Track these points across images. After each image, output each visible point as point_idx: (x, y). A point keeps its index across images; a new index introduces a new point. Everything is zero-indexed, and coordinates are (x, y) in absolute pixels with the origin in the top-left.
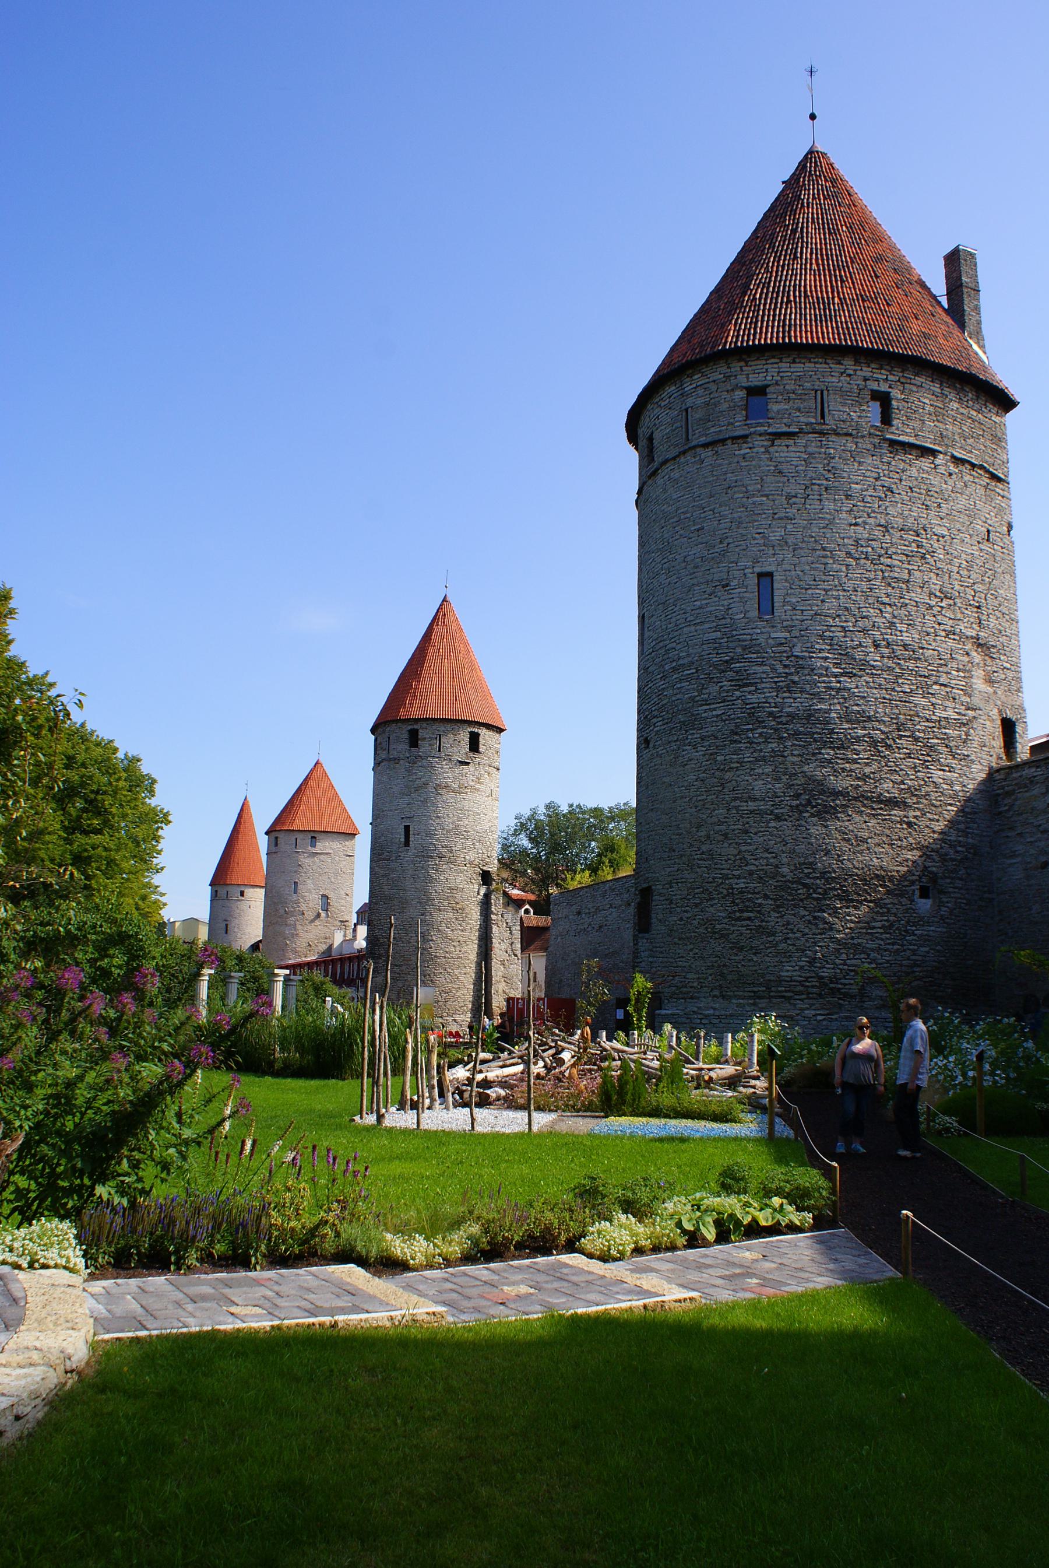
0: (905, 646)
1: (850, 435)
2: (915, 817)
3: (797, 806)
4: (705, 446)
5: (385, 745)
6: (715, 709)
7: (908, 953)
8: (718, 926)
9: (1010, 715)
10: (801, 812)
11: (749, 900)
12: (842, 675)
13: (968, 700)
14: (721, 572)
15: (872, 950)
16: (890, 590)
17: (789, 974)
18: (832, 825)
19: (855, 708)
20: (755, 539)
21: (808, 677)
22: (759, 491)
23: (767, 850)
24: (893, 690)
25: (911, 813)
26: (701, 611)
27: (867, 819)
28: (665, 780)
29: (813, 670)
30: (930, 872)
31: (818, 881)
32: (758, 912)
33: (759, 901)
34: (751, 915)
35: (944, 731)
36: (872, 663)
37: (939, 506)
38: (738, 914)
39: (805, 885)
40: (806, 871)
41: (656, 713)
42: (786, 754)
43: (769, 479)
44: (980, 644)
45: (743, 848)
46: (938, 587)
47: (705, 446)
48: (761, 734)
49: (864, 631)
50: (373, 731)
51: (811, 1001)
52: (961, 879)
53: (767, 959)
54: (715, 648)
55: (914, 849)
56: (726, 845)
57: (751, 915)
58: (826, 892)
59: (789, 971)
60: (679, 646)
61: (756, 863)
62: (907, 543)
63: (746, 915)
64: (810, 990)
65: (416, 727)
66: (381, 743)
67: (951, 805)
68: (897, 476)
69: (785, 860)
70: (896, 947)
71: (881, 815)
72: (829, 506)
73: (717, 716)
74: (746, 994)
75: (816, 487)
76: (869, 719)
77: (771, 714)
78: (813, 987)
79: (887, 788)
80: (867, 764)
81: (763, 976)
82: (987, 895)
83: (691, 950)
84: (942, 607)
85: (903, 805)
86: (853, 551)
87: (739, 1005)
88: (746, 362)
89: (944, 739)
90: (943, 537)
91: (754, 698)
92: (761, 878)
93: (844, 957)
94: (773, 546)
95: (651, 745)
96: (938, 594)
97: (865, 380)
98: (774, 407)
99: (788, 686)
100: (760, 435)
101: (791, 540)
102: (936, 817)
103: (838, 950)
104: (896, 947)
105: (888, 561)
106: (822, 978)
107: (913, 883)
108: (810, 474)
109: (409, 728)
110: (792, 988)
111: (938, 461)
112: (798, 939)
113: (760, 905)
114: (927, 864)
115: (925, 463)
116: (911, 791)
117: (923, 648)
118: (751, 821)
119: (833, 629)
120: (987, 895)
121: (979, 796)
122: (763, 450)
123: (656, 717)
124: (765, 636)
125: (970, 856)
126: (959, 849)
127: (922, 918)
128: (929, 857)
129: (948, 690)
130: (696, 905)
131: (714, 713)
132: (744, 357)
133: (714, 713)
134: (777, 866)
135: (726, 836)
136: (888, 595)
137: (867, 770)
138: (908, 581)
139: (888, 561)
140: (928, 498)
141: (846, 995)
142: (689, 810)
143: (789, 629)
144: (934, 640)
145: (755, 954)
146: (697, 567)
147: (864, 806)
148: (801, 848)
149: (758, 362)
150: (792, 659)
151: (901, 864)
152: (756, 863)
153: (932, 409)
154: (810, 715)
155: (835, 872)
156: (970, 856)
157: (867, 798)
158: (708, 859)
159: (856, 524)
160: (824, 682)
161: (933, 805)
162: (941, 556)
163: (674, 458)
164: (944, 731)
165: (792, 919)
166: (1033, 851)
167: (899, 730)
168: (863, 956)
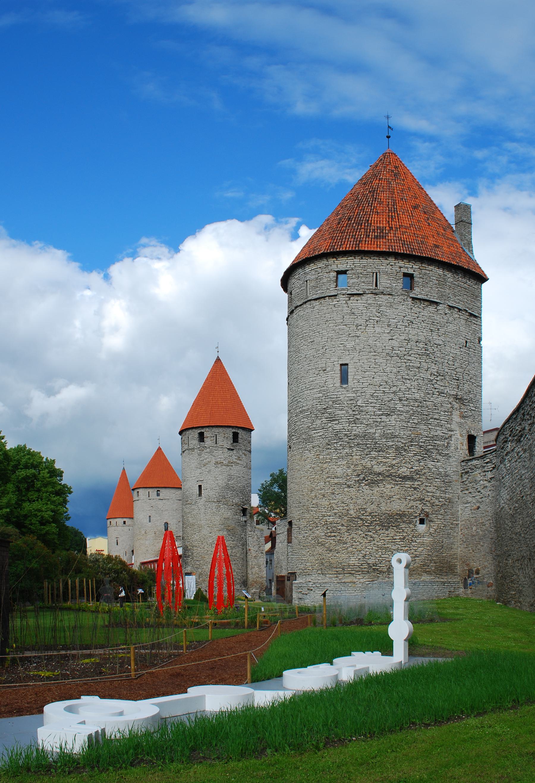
0: (416, 400)
2: (418, 485)
3: (358, 480)
5: (186, 442)
7: (412, 551)
8: (320, 540)
9: (473, 433)
10: (360, 483)
11: (334, 527)
12: (382, 415)
13: (449, 426)
15: (394, 550)
17: (353, 562)
18: (376, 489)
19: (388, 431)
20: (340, 347)
21: (365, 416)
22: (342, 323)
23: (343, 503)
24: (408, 422)
25: (416, 483)
27: (393, 486)
28: (297, 467)
29: (367, 413)
30: (426, 512)
31: (368, 517)
32: (339, 533)
33: (339, 527)
34: (336, 534)
35: (435, 442)
36: (398, 409)
38: (329, 534)
39: (361, 519)
40: (362, 512)
42: (353, 455)
43: (348, 316)
44: (456, 397)
45: (332, 502)
48: (341, 445)
49: (394, 393)
50: (181, 433)
51: (364, 575)
52: (442, 515)
53: (343, 555)
55: (417, 500)
56: (324, 500)
57: (336, 534)
58: (372, 522)
59: (353, 561)
60: (303, 400)
61: (338, 509)
63: (333, 534)
64: (363, 570)
65: (202, 431)
66: (184, 441)
67: (437, 478)
69: (352, 507)
70: (406, 548)
71: (400, 484)
72: (378, 330)
74: (333, 572)
76: (396, 436)
77: (346, 434)
78: (365, 568)
79: (404, 471)
80: (394, 459)
81: (341, 563)
82: (454, 522)
83: (308, 552)
85: (411, 478)
86: (390, 353)
87: (330, 578)
89: (435, 446)
91: (337, 427)
92: (340, 516)
93: (380, 553)
94: (349, 351)
99: (354, 421)
100: (343, 295)
101: (358, 348)
102: (430, 485)
103: (377, 550)
104: (406, 548)
106: (369, 564)
107: (416, 517)
108: (369, 314)
109: (199, 431)
110: (354, 569)
112: (357, 545)
113: (340, 529)
114: (423, 508)
116: (417, 472)
117: (425, 401)
118: (336, 488)
119: (377, 392)
120: (454, 522)
121: (453, 474)
122: (344, 302)
123: (293, 436)
124: (344, 396)
125: (446, 503)
126: (441, 500)
127: (420, 534)
128: (425, 504)
129: (438, 421)
130: (311, 530)
134: (348, 510)
135: (324, 496)
136: (408, 375)
137: (394, 462)
141: (381, 572)
142: (307, 483)
143: (356, 392)
145: (337, 553)
147: (392, 479)
148: (359, 502)
149: (343, 259)
150: (357, 407)
151: (410, 508)
152: (338, 509)
154: (365, 435)
155: (376, 512)
156: (446, 503)
157: (394, 476)
158: (315, 507)
159: (392, 339)
160: (373, 419)
161: (428, 479)
164: (435, 442)
165: (355, 536)
166: (474, 501)
167: (411, 442)
168: (389, 553)
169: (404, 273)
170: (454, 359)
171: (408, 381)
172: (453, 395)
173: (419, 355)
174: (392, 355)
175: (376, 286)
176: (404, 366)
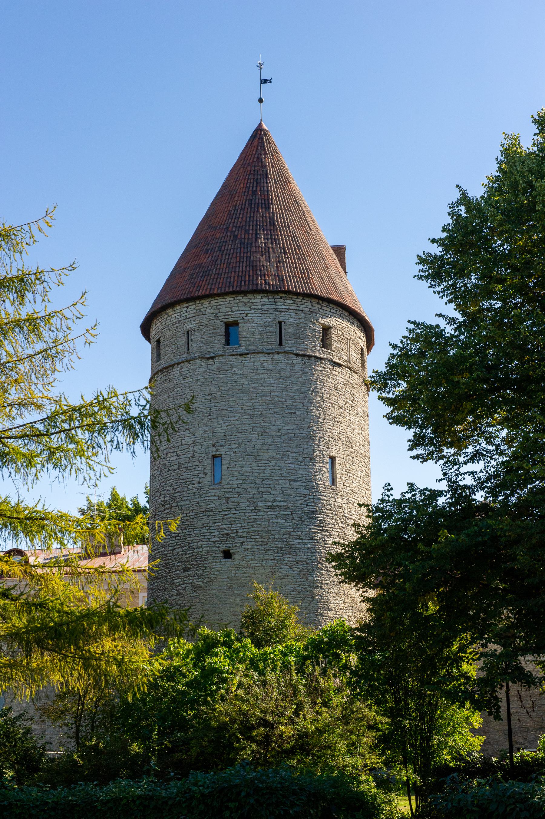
4: (298, 355)
6: (306, 543)
14: (309, 448)
26: (294, 472)
41: (245, 534)
47: (298, 355)
54: (305, 501)
73: (308, 548)
88: (322, 306)
95: (237, 557)
131: (306, 546)
132: (321, 302)
133: (306, 546)
146: (291, 440)
163: (269, 354)
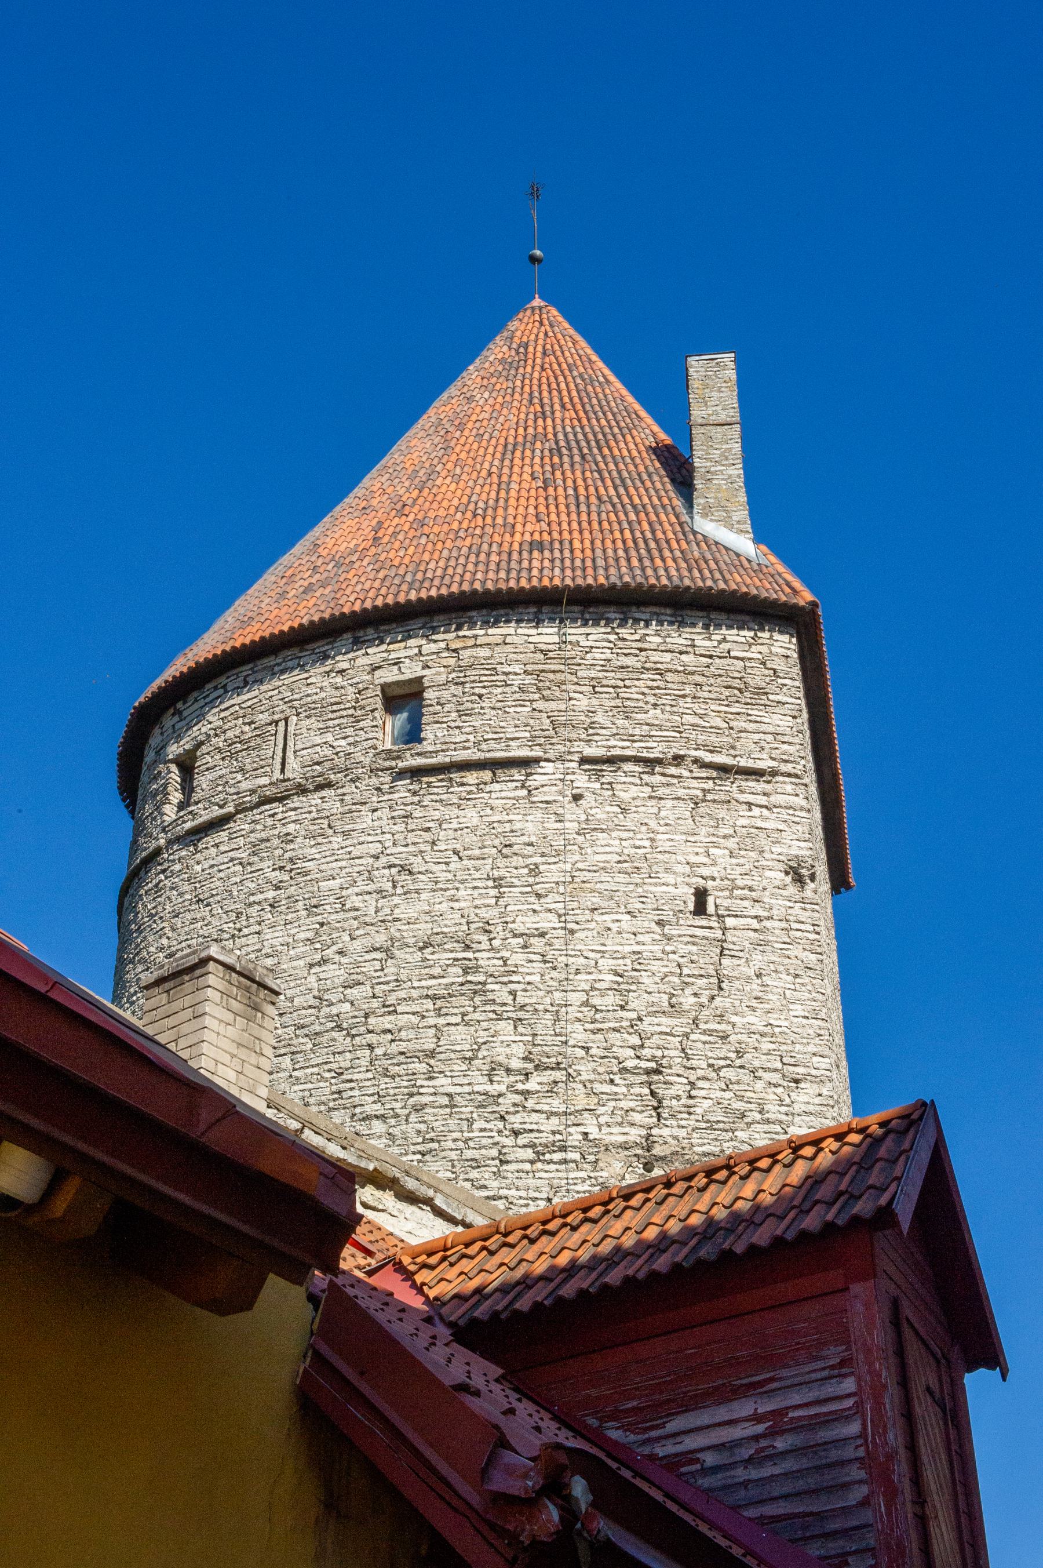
1: (329, 785)
16: (384, 1083)
37: (535, 871)
46: (519, 1050)
62: (436, 971)
68: (427, 836)
75: (253, 911)
84: (526, 1094)
90: (542, 935)
96: (516, 1064)
97: (375, 668)
98: (203, 781)
105: (387, 1022)
111: (537, 780)
115: (505, 789)
136: (379, 1097)
138: (432, 1054)
139: (387, 1022)
140: (501, 862)
144: (497, 1174)
153: (528, 680)
162: (536, 978)
169: (384, 687)
170: (624, 983)
171: (378, 1127)
172: (625, 1146)
173: (434, 998)
174: (317, 1028)
175: (283, 771)
176: (364, 1062)
